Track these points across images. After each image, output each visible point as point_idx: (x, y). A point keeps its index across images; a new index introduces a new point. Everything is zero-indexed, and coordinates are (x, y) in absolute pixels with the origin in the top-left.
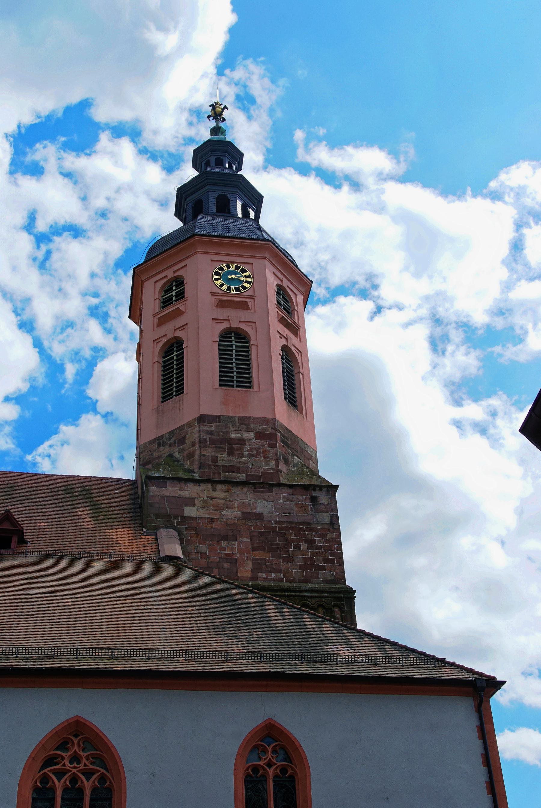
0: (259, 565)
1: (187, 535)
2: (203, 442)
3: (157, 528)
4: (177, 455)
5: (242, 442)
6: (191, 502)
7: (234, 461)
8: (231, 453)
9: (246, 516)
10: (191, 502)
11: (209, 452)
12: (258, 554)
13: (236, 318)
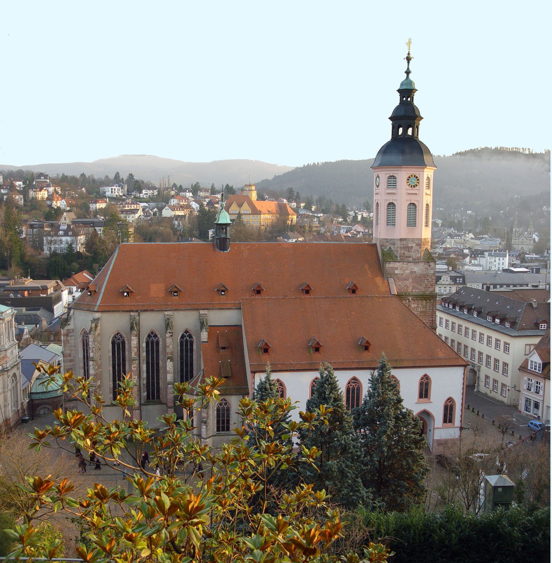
0: (413, 288)
1: (396, 279)
2: (401, 248)
3: (388, 278)
4: (392, 248)
5: (412, 247)
6: (397, 269)
7: (409, 254)
8: (408, 252)
9: (411, 272)
10: (397, 269)
11: (403, 252)
12: (414, 284)
13: (413, 199)
